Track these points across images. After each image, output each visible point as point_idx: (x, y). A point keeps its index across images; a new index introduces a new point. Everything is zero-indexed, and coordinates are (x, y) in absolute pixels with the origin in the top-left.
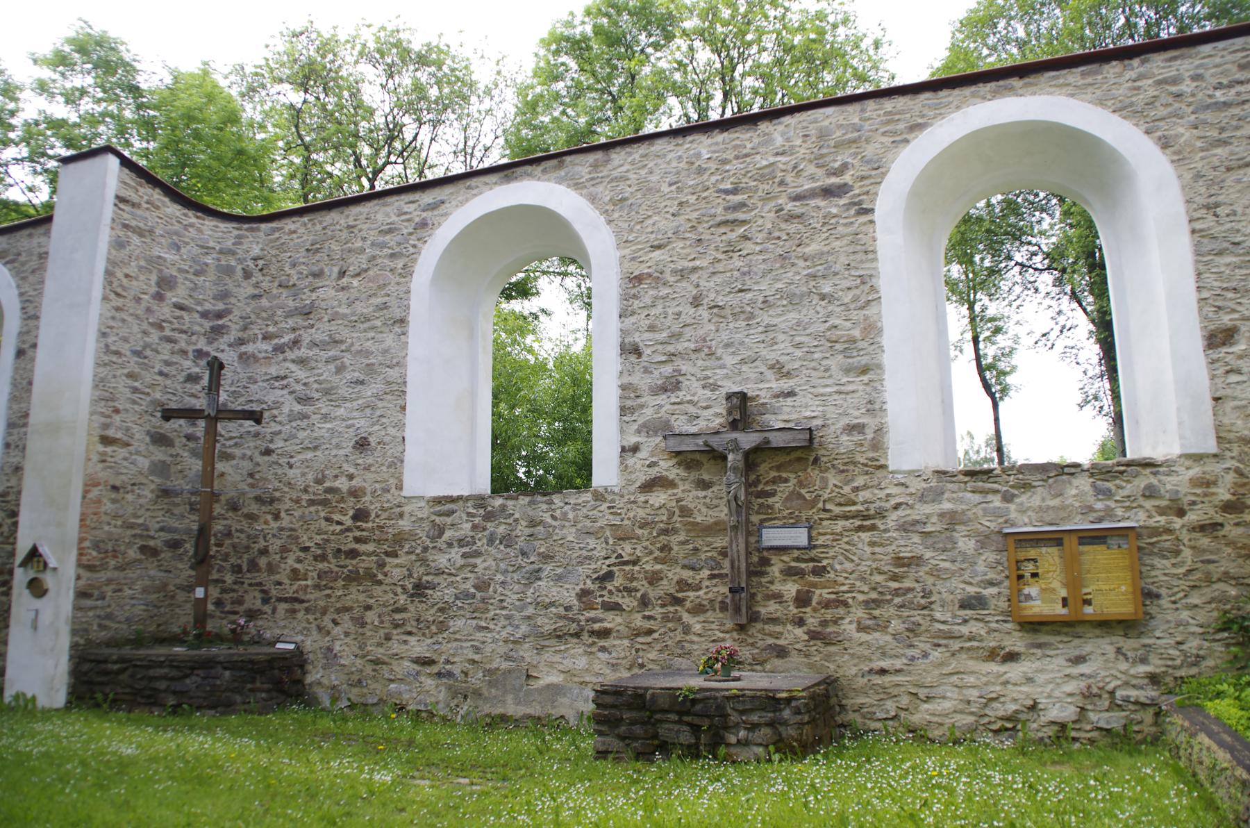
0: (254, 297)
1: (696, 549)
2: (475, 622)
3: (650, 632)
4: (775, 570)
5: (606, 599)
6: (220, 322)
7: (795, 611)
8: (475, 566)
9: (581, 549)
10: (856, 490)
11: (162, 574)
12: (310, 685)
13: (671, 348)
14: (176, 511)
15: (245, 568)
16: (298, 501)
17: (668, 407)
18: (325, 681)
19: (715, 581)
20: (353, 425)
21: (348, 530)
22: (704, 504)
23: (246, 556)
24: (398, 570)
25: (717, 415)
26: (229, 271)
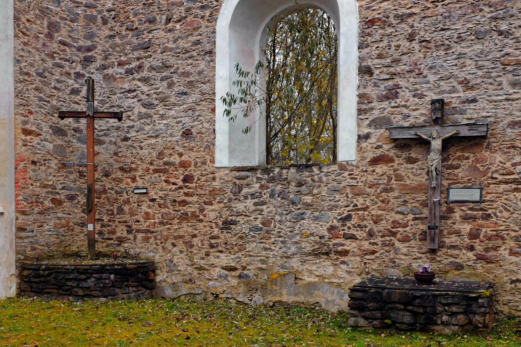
0: (111, 37)
1: (405, 201)
2: (262, 245)
3: (373, 252)
4: (457, 215)
5: (346, 232)
6: (90, 54)
7: (468, 241)
8: (262, 211)
9: (330, 200)
10: (514, 165)
11: (65, 216)
12: (160, 282)
13: (392, 70)
14: (72, 177)
15: (115, 212)
16: (148, 170)
17: (389, 109)
18: (169, 280)
19: (416, 222)
20: (181, 122)
21: (181, 188)
22: (412, 172)
23: (115, 205)
24: (213, 213)
25: (422, 115)
26: (92, 19)
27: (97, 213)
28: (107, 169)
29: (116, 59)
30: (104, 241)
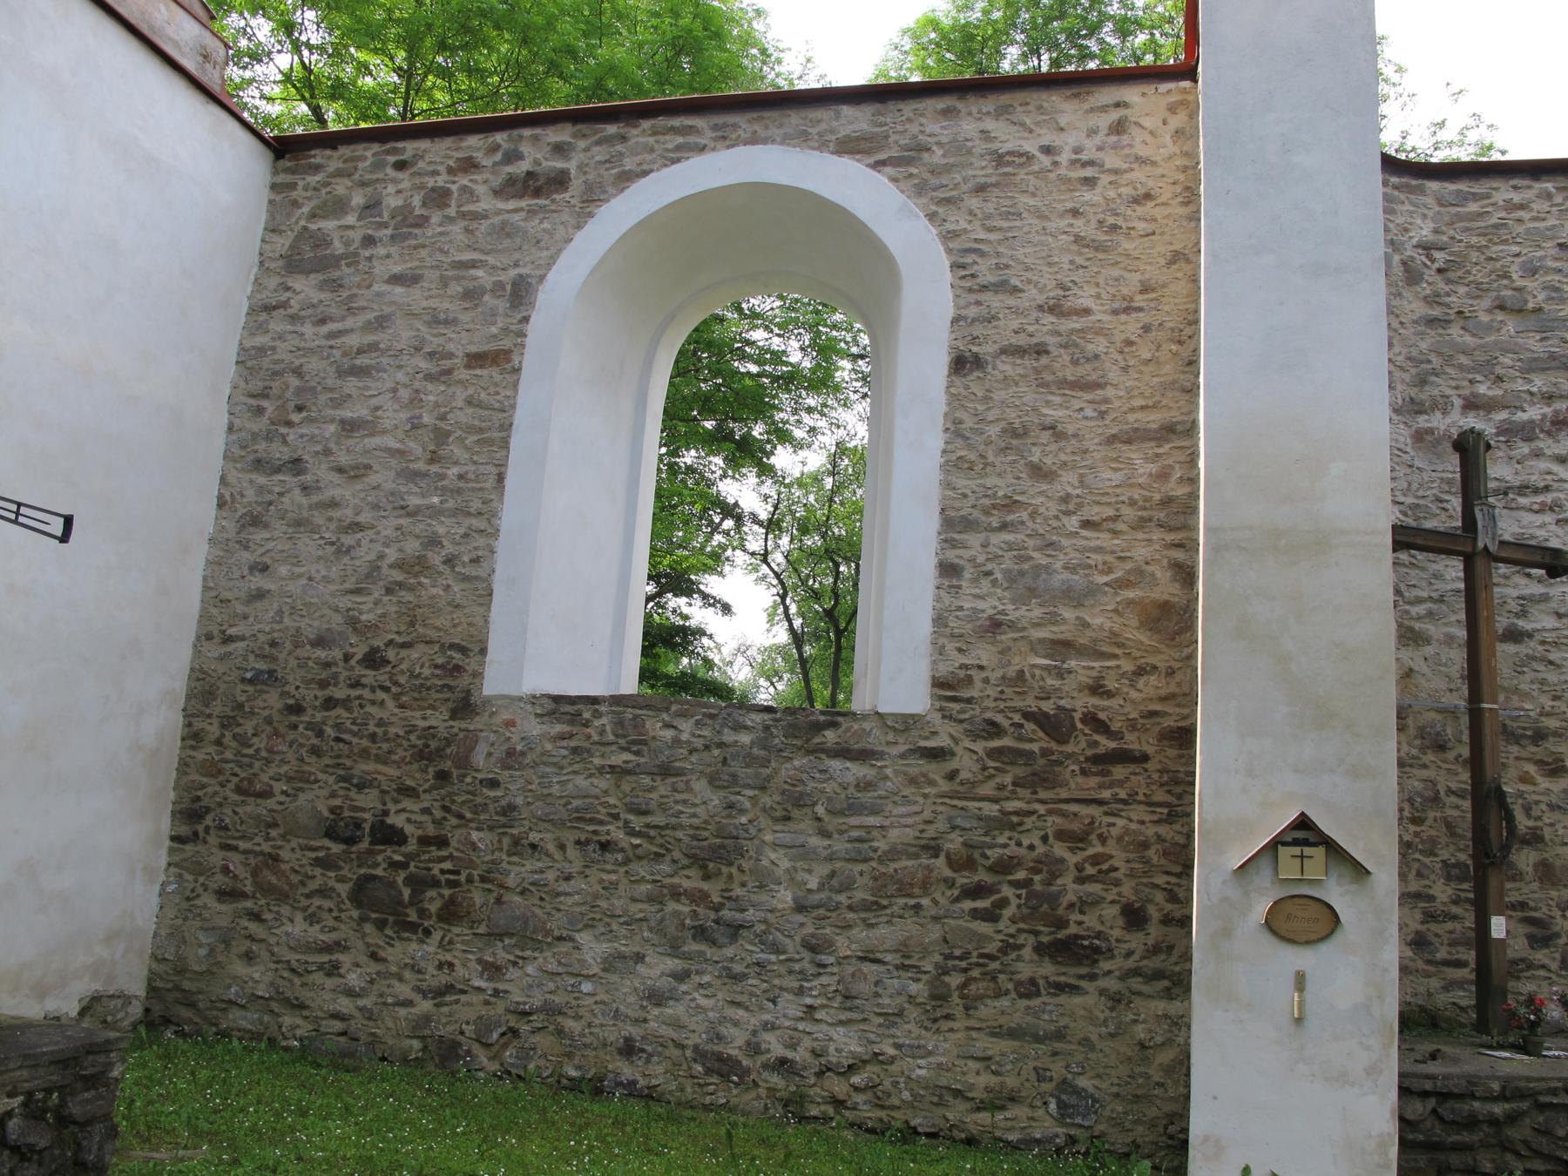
0: (1431, 322)
27: (1414, 872)
28: (1438, 728)
29: (1457, 388)
30: (1432, 969)
